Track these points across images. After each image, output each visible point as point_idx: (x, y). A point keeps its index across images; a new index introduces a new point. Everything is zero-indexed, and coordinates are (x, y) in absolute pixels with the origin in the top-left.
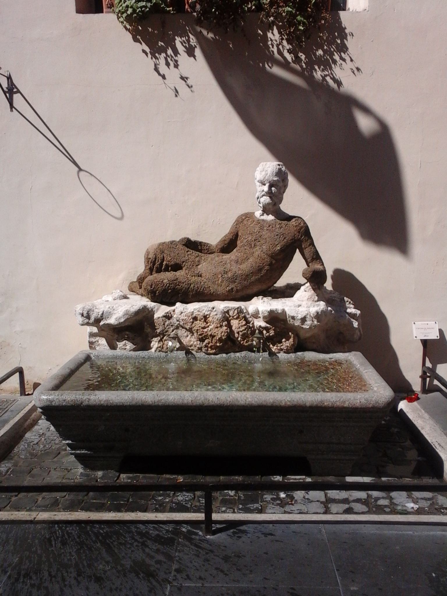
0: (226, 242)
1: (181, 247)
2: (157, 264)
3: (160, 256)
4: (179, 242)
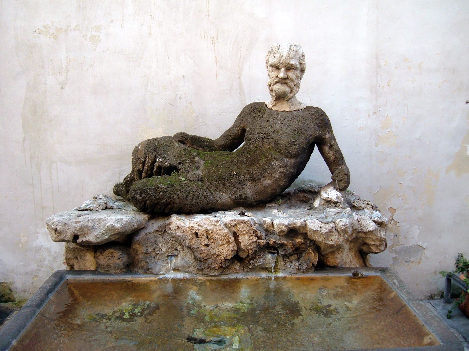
0: (230, 138)
1: (176, 144)
2: (148, 164)
3: (151, 156)
4: (173, 138)
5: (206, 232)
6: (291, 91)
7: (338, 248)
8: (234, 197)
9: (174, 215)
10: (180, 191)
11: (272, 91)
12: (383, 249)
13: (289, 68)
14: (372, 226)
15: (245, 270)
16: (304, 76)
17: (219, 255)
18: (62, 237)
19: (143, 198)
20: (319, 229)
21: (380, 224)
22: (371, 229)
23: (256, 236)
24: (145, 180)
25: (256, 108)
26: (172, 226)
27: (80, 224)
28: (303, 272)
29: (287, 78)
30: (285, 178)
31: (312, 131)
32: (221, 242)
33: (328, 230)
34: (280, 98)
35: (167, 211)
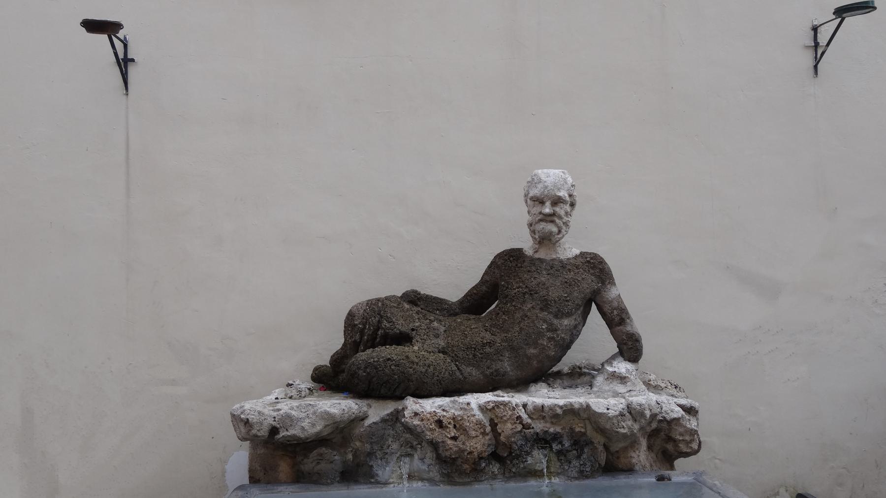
1: (407, 306)
3: (375, 320)
4: (401, 297)
5: (454, 419)
6: (560, 232)
7: (632, 442)
8: (488, 372)
9: (409, 397)
10: (417, 364)
11: (533, 232)
12: (696, 447)
13: (557, 201)
14: (678, 413)
15: (507, 475)
16: (574, 213)
17: (470, 453)
18: (254, 432)
19: (368, 373)
20: (605, 411)
21: (690, 411)
22: (675, 416)
23: (521, 423)
24: (369, 351)
25: (512, 256)
26: (407, 413)
27: (281, 412)
28: (587, 477)
29: (554, 214)
30: (555, 346)
31: (589, 282)
32: (474, 432)
33: (617, 413)
34: (545, 240)
35: (398, 393)
